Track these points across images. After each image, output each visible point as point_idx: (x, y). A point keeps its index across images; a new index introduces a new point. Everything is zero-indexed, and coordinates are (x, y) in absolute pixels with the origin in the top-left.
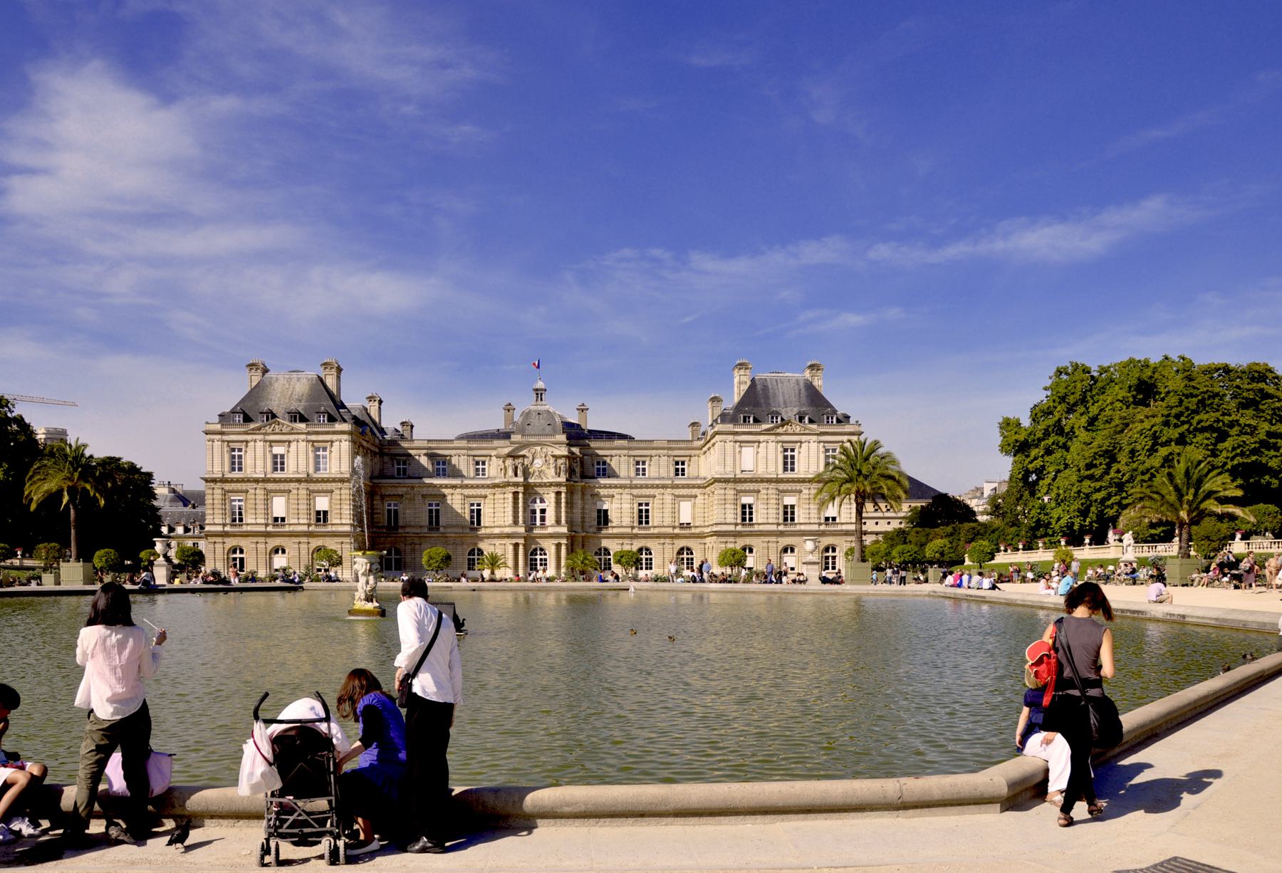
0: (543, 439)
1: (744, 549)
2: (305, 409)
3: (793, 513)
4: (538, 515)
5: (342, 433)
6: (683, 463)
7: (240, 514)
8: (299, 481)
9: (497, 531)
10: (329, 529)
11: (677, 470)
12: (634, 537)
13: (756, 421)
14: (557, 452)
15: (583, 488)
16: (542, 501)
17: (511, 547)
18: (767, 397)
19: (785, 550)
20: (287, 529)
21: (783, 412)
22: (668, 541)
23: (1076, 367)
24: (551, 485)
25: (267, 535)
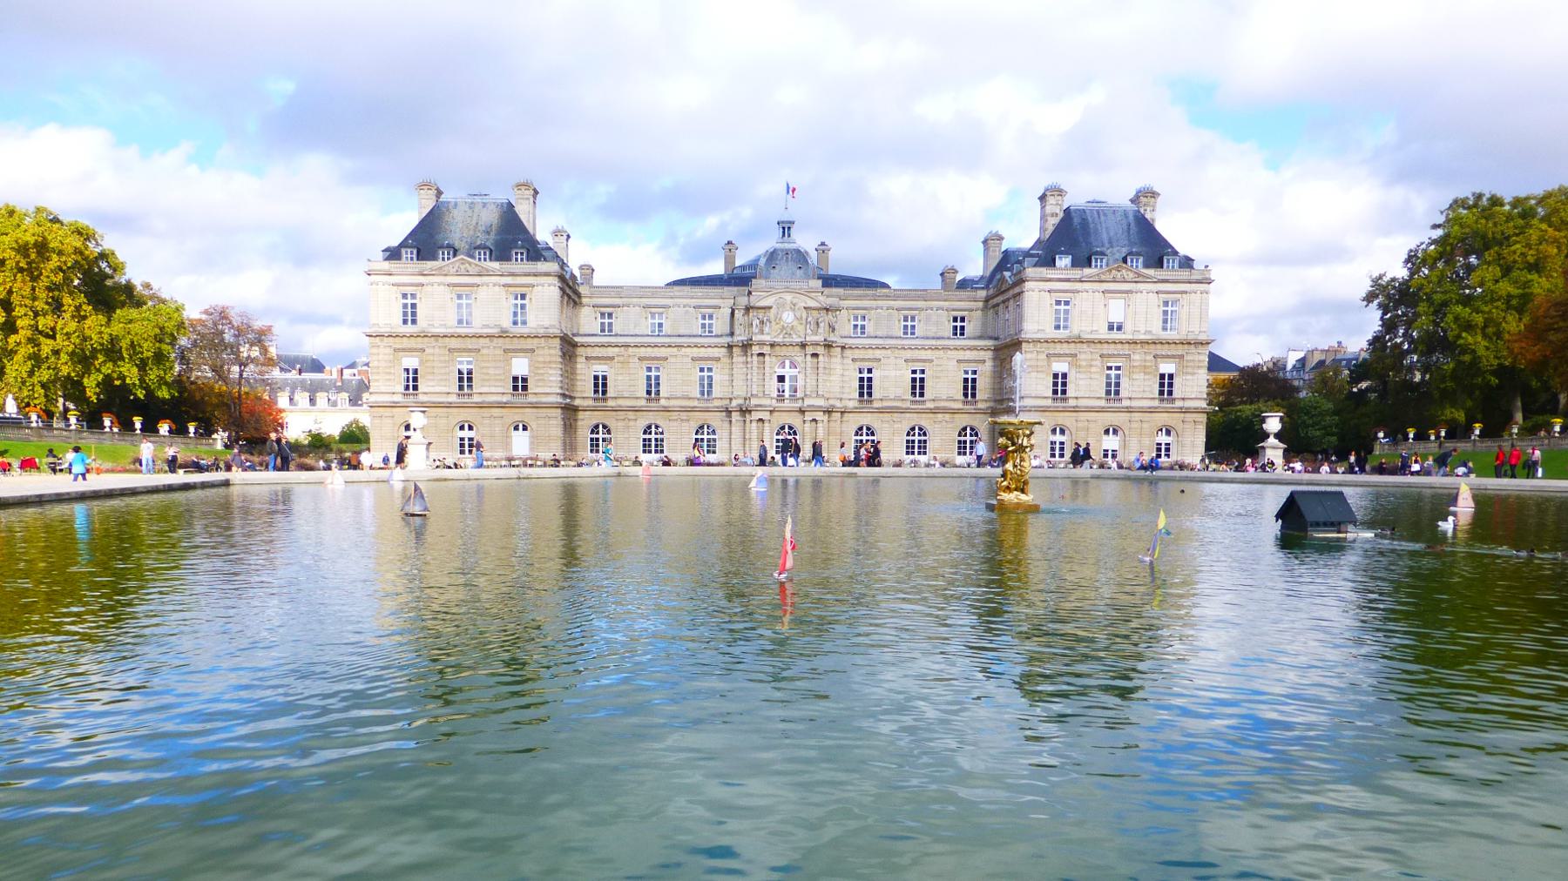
0: (794, 285)
1: (1054, 431)
3: (1117, 385)
5: (547, 274)
6: (963, 320)
9: (734, 403)
10: (532, 399)
11: (955, 328)
12: (903, 411)
13: (1075, 264)
15: (843, 348)
16: (793, 366)
19: (1107, 432)
20: (476, 399)
23: (1479, 197)
24: (803, 346)
25: (449, 406)
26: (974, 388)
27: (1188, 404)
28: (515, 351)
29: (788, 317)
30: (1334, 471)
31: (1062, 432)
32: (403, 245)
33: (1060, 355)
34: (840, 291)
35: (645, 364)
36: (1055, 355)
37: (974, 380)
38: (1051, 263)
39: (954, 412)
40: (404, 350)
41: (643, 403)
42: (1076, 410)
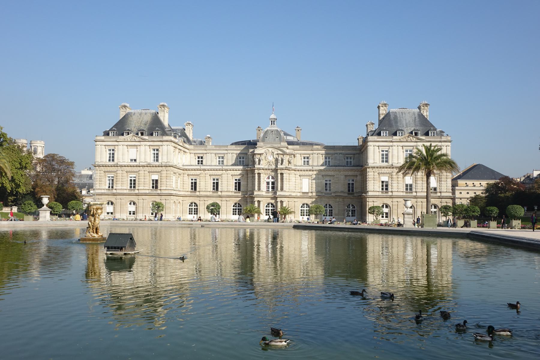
2: (149, 129)
3: (411, 185)
4: (270, 185)
7: (113, 184)
8: (144, 166)
9: (249, 193)
10: (159, 192)
14: (281, 153)
16: (273, 178)
17: (256, 203)
18: (396, 122)
20: (137, 192)
21: (405, 130)
22: (341, 200)
26: (353, 188)
27: (443, 194)
28: (154, 172)
29: (271, 159)
30: (466, 225)
31: (387, 207)
32: (111, 130)
33: (384, 173)
34: (298, 147)
35: (212, 177)
36: (382, 173)
37: (353, 184)
38: (379, 134)
39: (344, 197)
40: (108, 172)
41: (211, 193)
42: (391, 197)
